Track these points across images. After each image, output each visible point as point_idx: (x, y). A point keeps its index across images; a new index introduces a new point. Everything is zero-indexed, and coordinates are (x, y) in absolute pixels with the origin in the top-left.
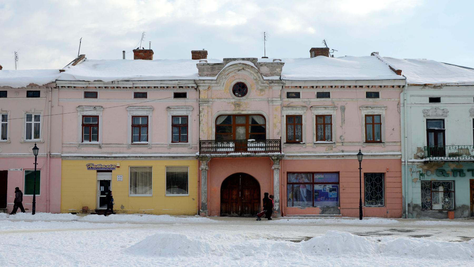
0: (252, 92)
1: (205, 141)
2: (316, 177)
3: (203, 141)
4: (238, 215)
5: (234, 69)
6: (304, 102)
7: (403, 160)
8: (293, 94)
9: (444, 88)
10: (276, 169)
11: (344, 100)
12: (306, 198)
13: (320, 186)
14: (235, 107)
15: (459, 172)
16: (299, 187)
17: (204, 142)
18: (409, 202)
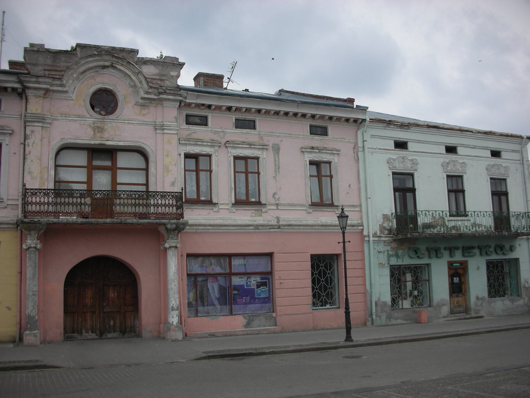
1: (36, 191)
2: (236, 262)
3: (32, 191)
4: (97, 335)
5: (95, 64)
6: (216, 133)
7: (365, 233)
8: (197, 118)
9: (412, 129)
10: (173, 247)
11: (278, 135)
12: (218, 299)
13: (241, 278)
14: (94, 132)
15: (436, 252)
16: (207, 280)
17: (35, 192)
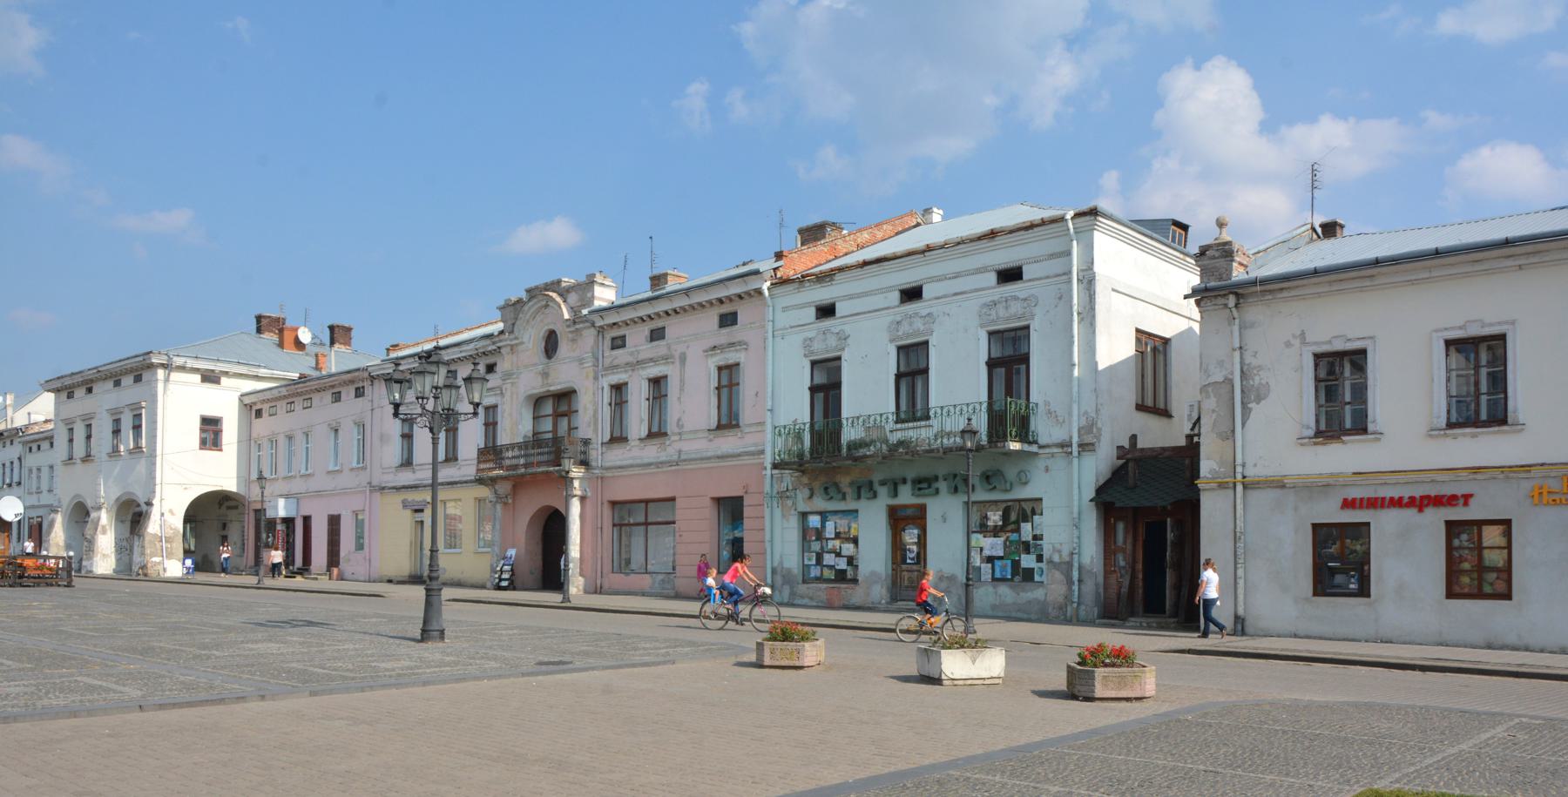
0: (564, 349)
5: (536, 306)
15: (865, 489)
18: (775, 564)
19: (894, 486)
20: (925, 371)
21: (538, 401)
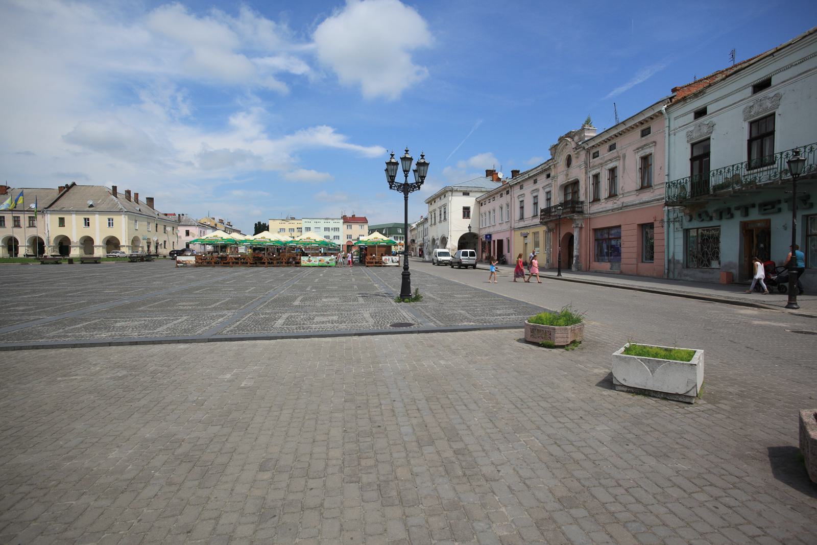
0: (574, 162)
15: (725, 213)
19: (746, 211)
20: (772, 133)
21: (565, 187)
